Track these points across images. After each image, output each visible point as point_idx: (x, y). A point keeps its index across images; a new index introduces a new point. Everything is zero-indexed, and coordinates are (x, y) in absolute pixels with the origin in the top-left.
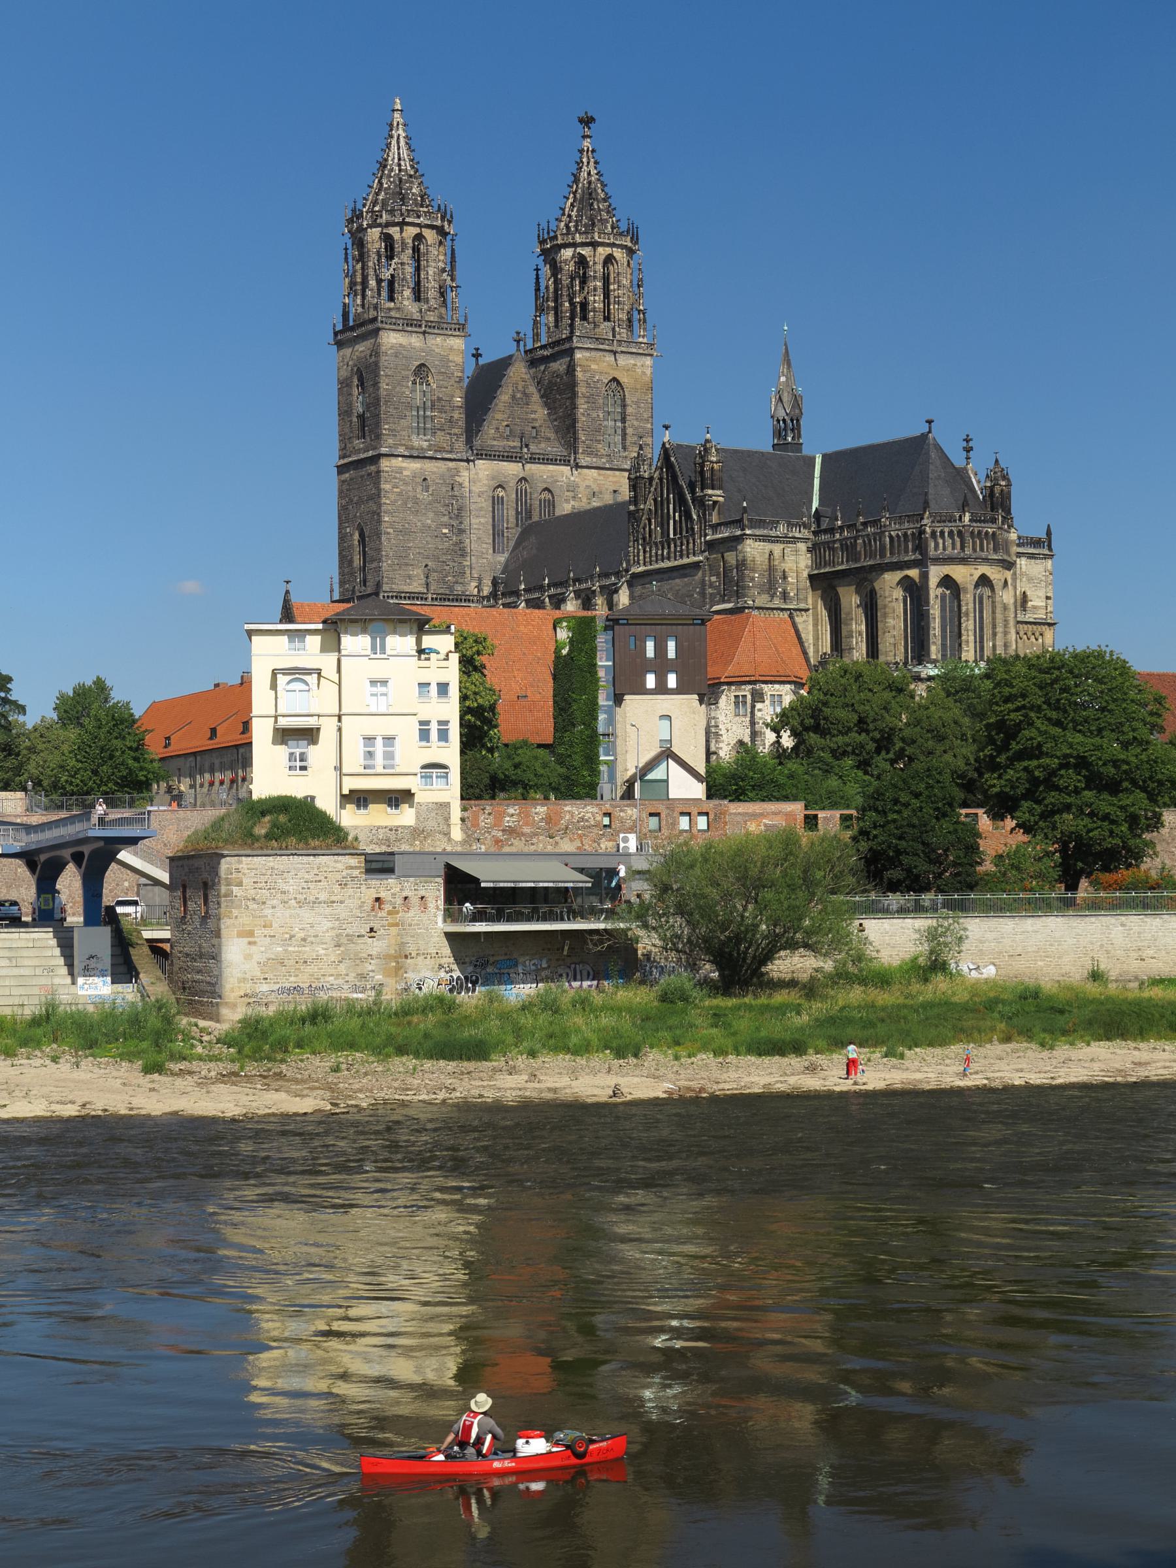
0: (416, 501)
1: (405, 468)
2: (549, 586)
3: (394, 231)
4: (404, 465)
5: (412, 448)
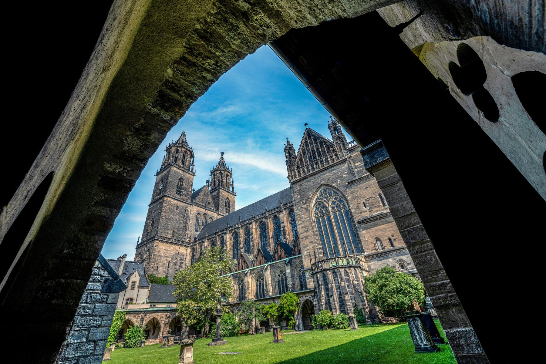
0: (174, 211)
1: (172, 201)
2: (218, 232)
3: (180, 149)
4: (172, 200)
5: (175, 197)
